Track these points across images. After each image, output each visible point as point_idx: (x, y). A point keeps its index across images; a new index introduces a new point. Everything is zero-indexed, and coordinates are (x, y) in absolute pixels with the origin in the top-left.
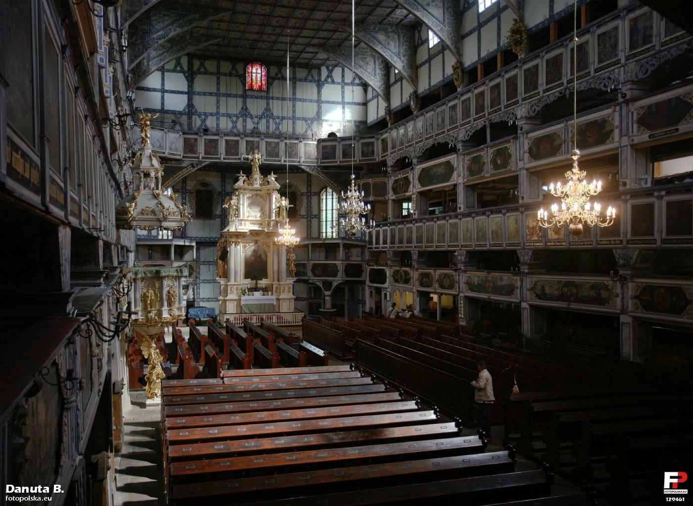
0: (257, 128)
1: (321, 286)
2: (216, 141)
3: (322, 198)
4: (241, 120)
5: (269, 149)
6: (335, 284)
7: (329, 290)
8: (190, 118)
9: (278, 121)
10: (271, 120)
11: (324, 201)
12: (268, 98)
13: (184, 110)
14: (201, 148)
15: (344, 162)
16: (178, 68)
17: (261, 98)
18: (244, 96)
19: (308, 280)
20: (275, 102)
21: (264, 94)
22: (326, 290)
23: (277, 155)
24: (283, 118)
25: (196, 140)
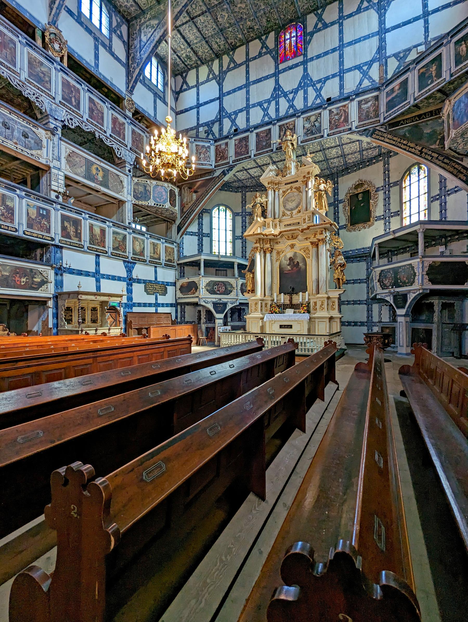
0: (292, 106)
1: (392, 302)
2: (246, 138)
3: (404, 186)
4: (273, 103)
5: (307, 125)
6: (411, 297)
7: (403, 307)
8: (221, 124)
9: (318, 86)
10: (310, 89)
11: (408, 188)
12: (304, 63)
13: (217, 116)
14: (231, 152)
15: (422, 95)
16: (211, 76)
17: (296, 65)
18: (276, 75)
19: (376, 295)
20: (315, 62)
21: (300, 59)
22: (398, 308)
23: (319, 130)
24: (327, 78)
25: (227, 144)
